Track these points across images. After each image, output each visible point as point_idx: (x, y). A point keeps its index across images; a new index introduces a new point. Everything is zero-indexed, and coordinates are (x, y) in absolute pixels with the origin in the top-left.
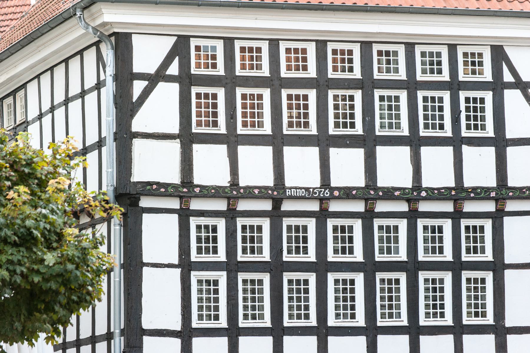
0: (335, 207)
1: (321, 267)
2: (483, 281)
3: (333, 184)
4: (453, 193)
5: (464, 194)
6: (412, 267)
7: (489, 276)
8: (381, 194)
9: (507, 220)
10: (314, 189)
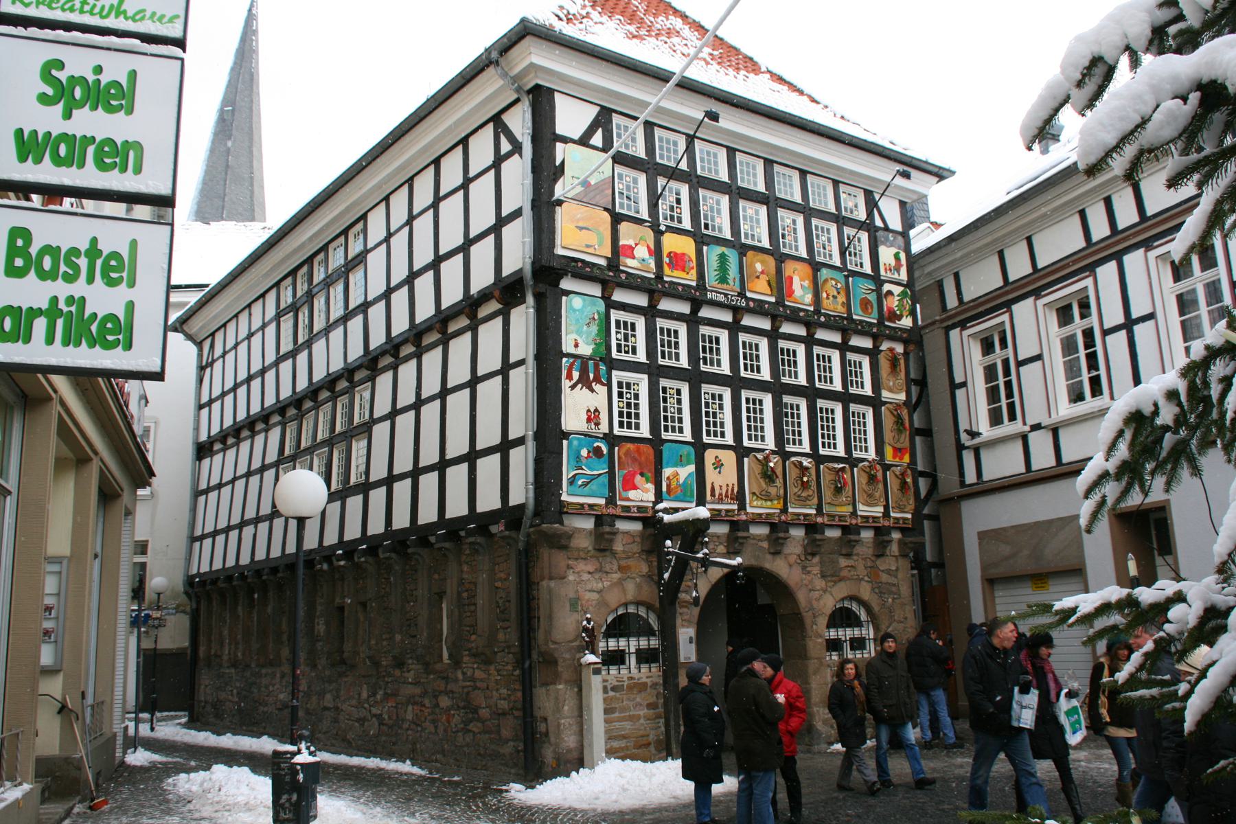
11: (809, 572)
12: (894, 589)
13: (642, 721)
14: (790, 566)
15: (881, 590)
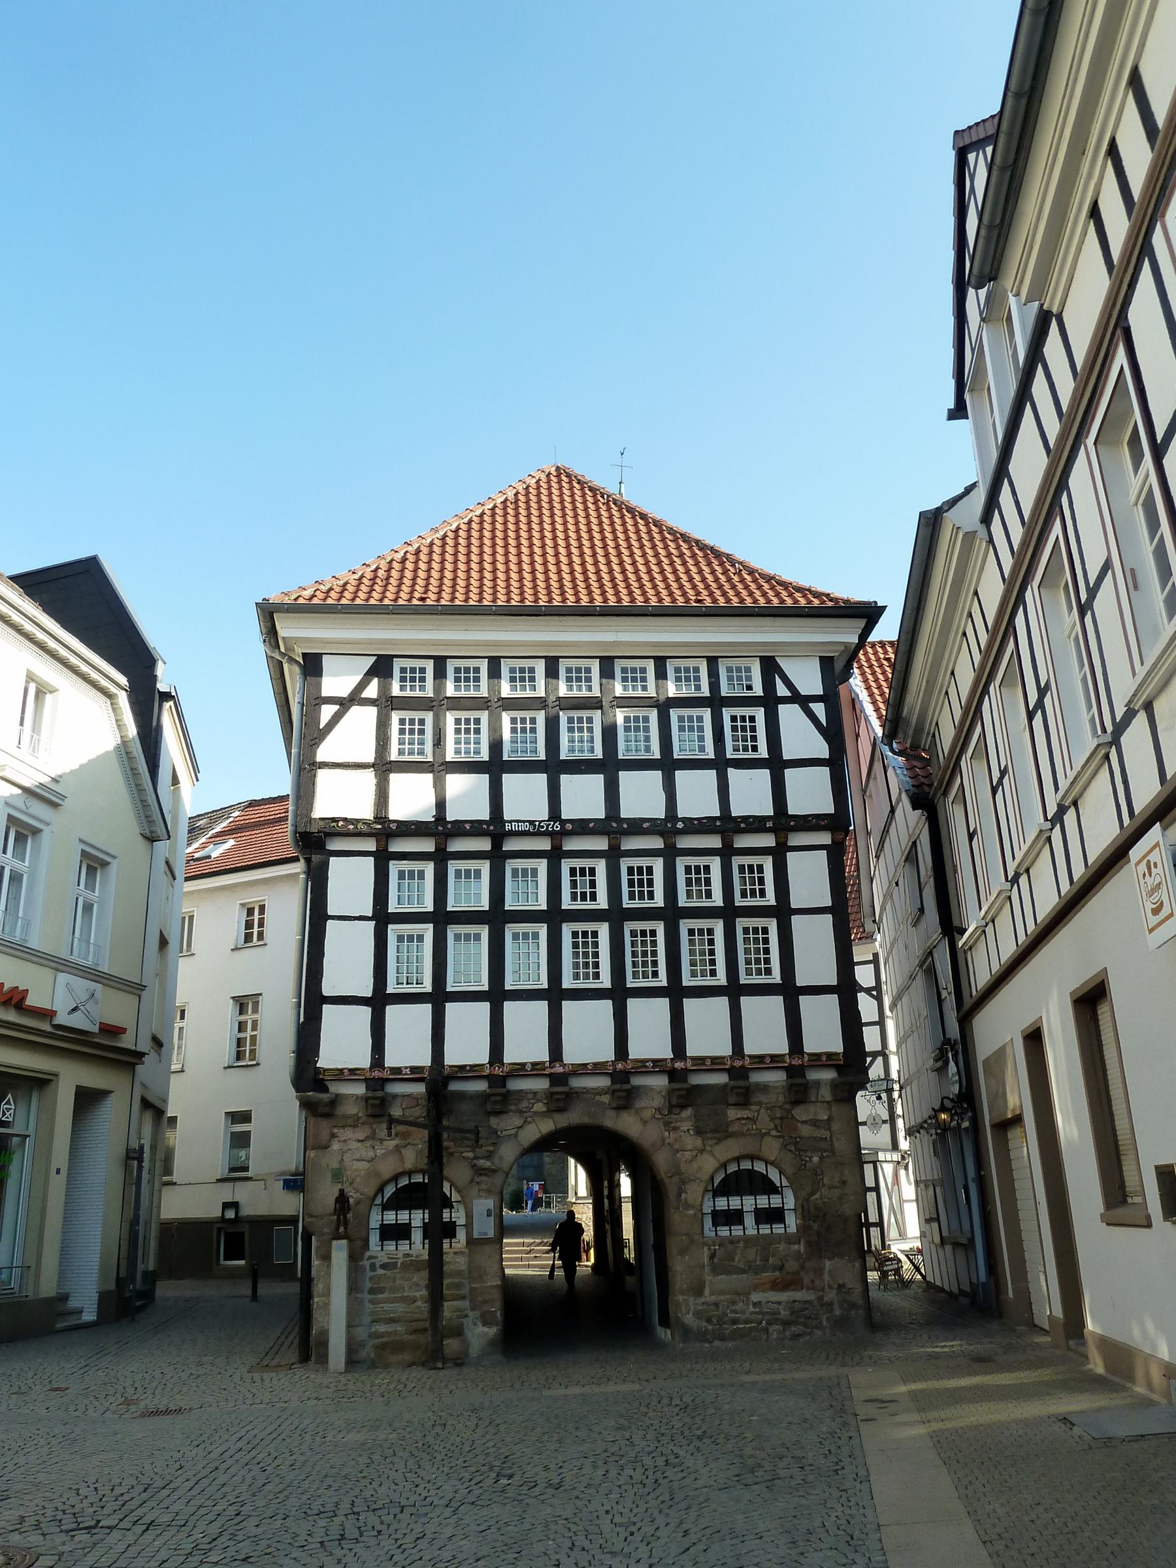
0: (571, 845)
1: (554, 916)
2: (765, 931)
3: (565, 816)
4: (718, 823)
5: (732, 825)
6: (671, 914)
7: (773, 925)
8: (625, 826)
9: (791, 857)
10: (541, 822)
11: (675, 1129)
12: (823, 1145)
13: (419, 1303)
14: (645, 1122)
15: (795, 1145)
